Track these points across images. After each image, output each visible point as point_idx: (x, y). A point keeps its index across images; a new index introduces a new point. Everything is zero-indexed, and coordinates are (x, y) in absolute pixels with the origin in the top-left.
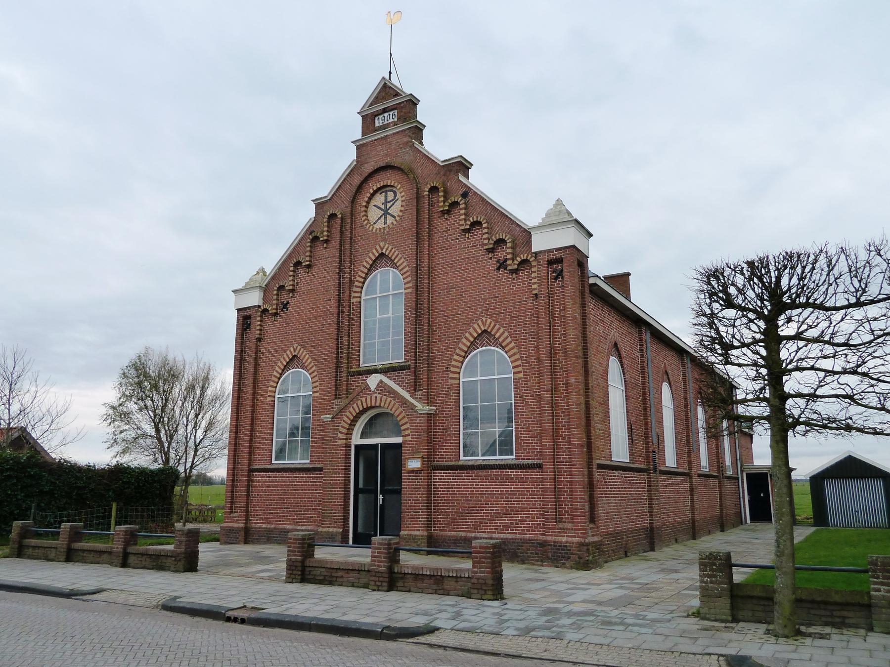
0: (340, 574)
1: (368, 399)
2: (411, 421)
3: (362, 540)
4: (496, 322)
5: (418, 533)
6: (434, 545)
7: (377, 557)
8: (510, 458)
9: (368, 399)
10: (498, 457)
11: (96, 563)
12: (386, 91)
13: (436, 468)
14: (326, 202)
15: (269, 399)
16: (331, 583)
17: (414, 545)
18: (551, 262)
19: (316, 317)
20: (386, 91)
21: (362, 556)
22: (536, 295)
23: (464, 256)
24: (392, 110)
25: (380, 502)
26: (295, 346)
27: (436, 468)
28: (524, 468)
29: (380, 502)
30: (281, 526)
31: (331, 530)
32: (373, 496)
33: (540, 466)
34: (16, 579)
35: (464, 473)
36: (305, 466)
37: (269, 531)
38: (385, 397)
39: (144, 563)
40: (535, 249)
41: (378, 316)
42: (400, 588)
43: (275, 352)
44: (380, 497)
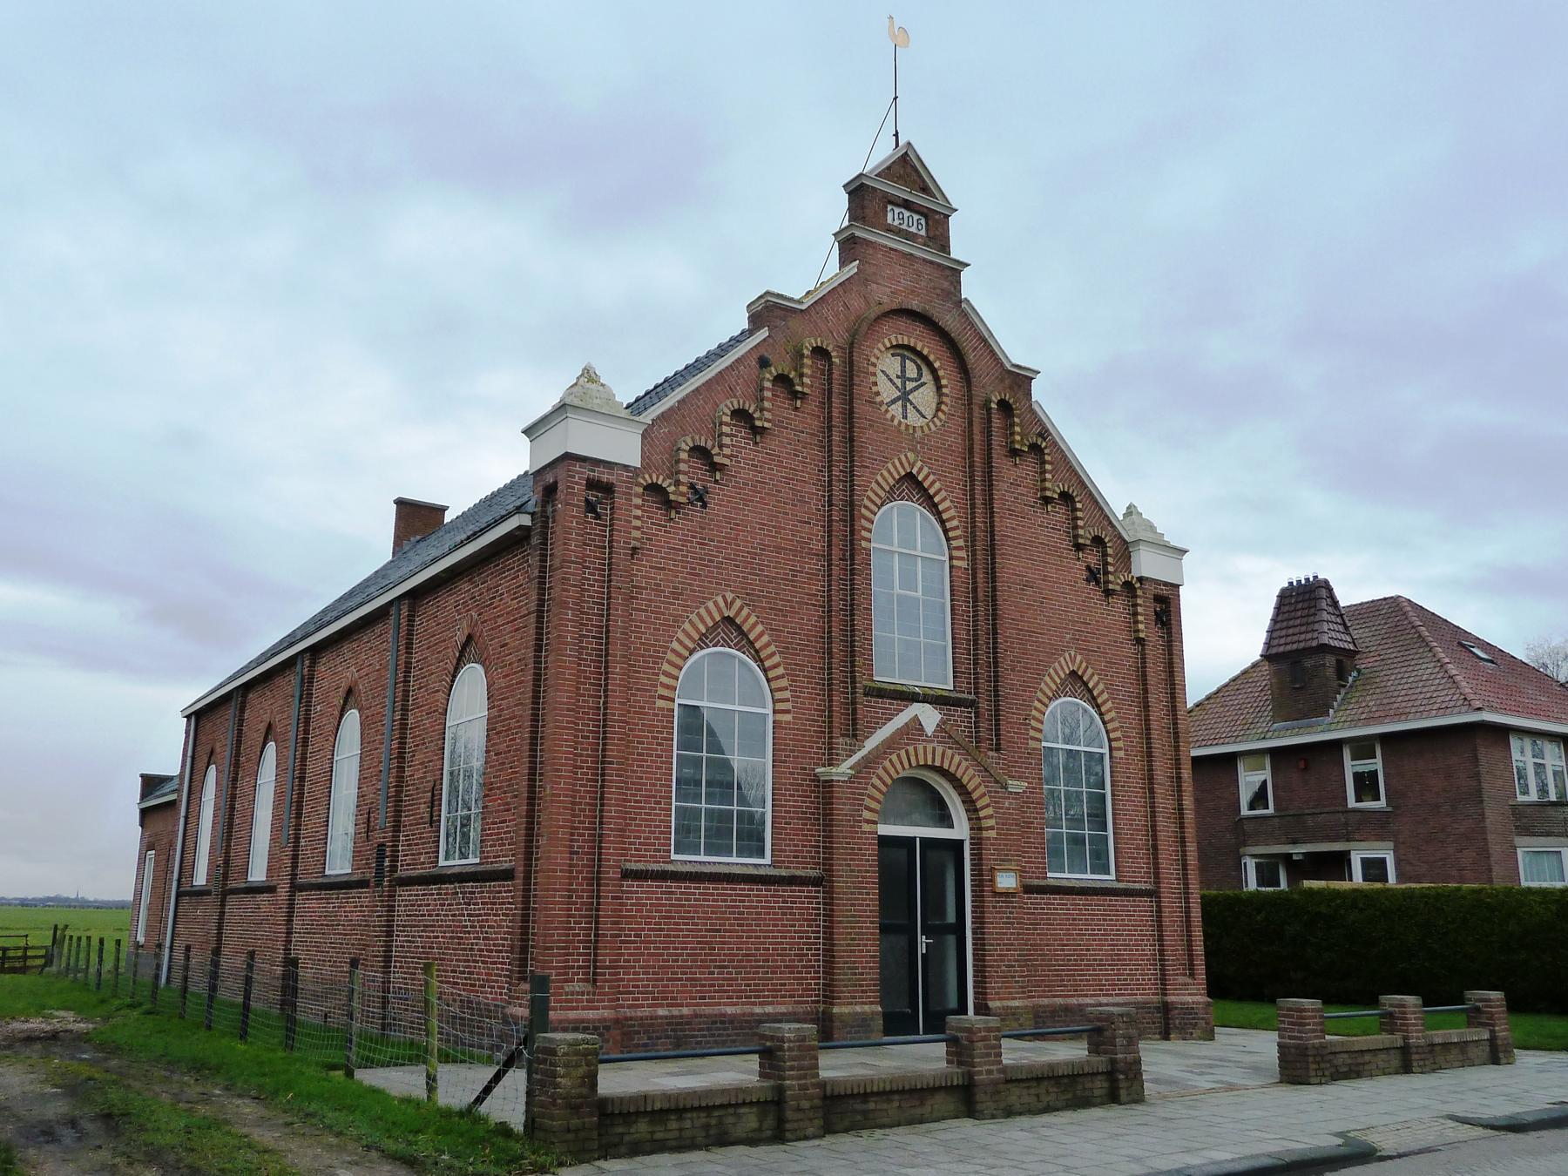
0: (1367, 1058)
1: (921, 751)
2: (996, 804)
3: (898, 1024)
4: (1088, 662)
5: (1016, 1003)
6: (1044, 1025)
7: (994, 1047)
8: (1109, 878)
9: (921, 751)
10: (734, 859)
11: (910, 1122)
12: (906, 168)
13: (816, 882)
14: (794, 310)
15: (660, 703)
16: (1358, 1075)
17: (1015, 1025)
18: (592, 484)
19: (779, 549)
20: (906, 168)
21: (925, 1058)
22: (634, 549)
23: (1042, 539)
24: (896, 204)
25: (922, 950)
26: (730, 596)
27: (816, 882)
28: (773, 884)
29: (922, 950)
30: (708, 1010)
31: (858, 1009)
32: (902, 941)
33: (627, 875)
34: (1247, 1151)
35: (1056, 899)
36: (762, 872)
37: (677, 1023)
38: (949, 752)
39: (1045, 1099)
40: (636, 462)
41: (897, 590)
42: (1313, 1080)
43: (676, 595)
44: (923, 942)
